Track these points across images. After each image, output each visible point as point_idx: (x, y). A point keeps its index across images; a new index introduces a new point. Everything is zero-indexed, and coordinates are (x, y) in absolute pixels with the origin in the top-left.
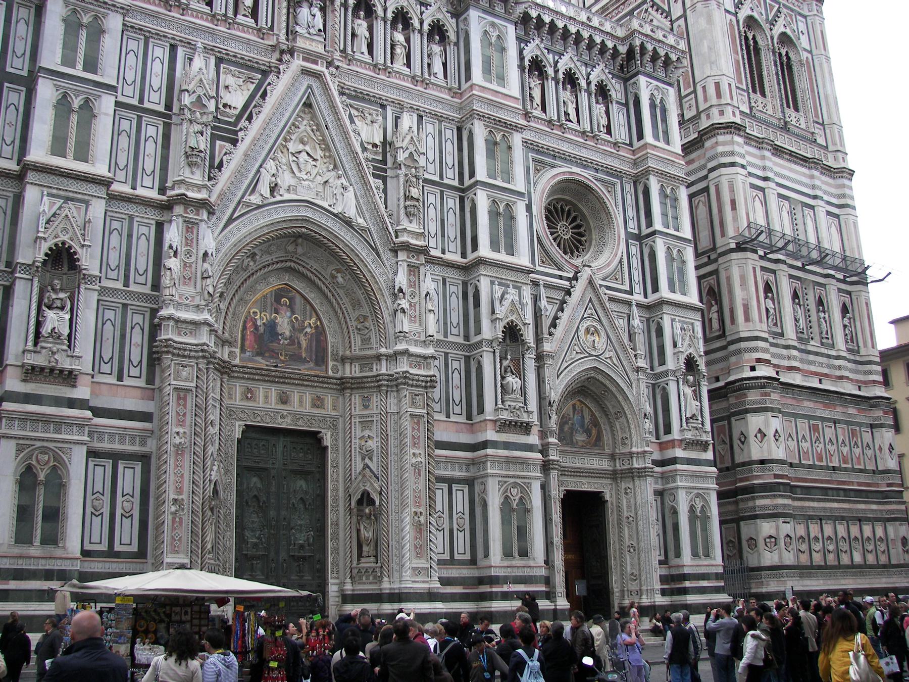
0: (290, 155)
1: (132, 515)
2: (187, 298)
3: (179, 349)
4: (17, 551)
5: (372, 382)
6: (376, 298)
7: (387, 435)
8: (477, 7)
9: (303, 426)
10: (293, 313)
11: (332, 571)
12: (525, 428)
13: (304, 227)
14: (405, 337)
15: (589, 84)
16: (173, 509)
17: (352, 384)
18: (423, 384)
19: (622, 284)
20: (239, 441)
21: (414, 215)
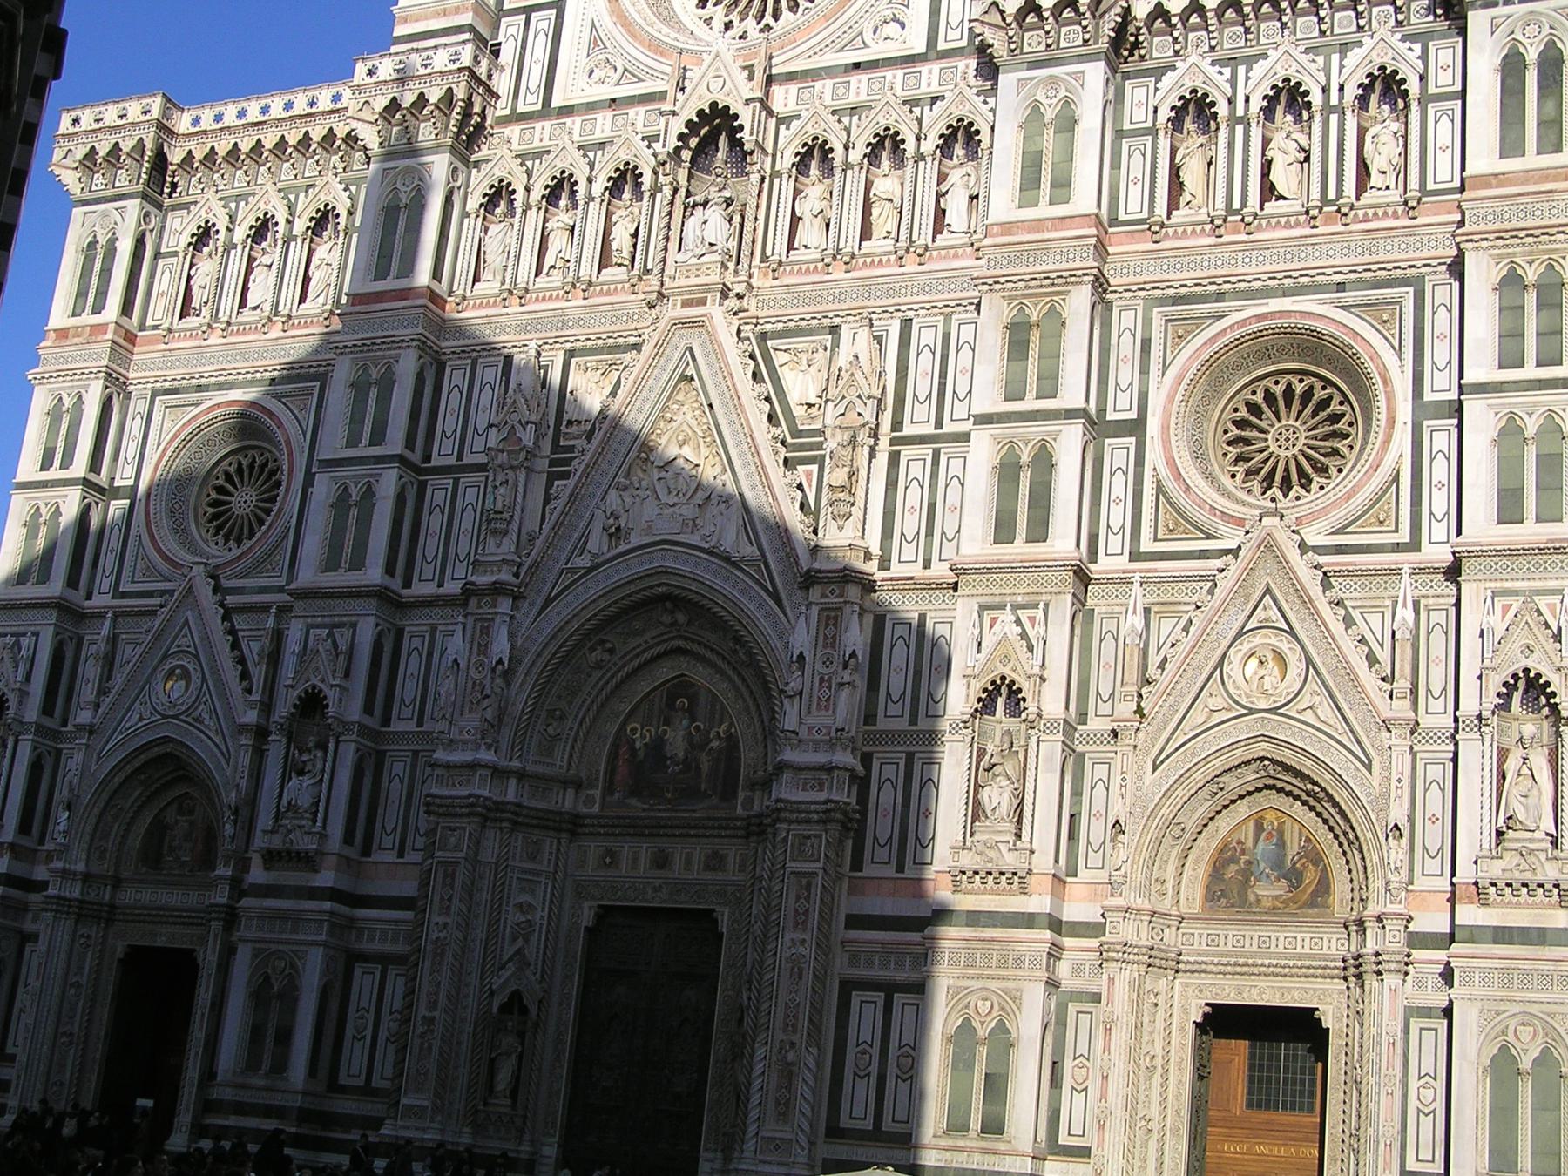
0: (656, 470)
8: (1014, 67)
9: (686, 902)
10: (693, 719)
15: (1341, 88)
16: (421, 1029)
18: (815, 817)
19: (1396, 531)
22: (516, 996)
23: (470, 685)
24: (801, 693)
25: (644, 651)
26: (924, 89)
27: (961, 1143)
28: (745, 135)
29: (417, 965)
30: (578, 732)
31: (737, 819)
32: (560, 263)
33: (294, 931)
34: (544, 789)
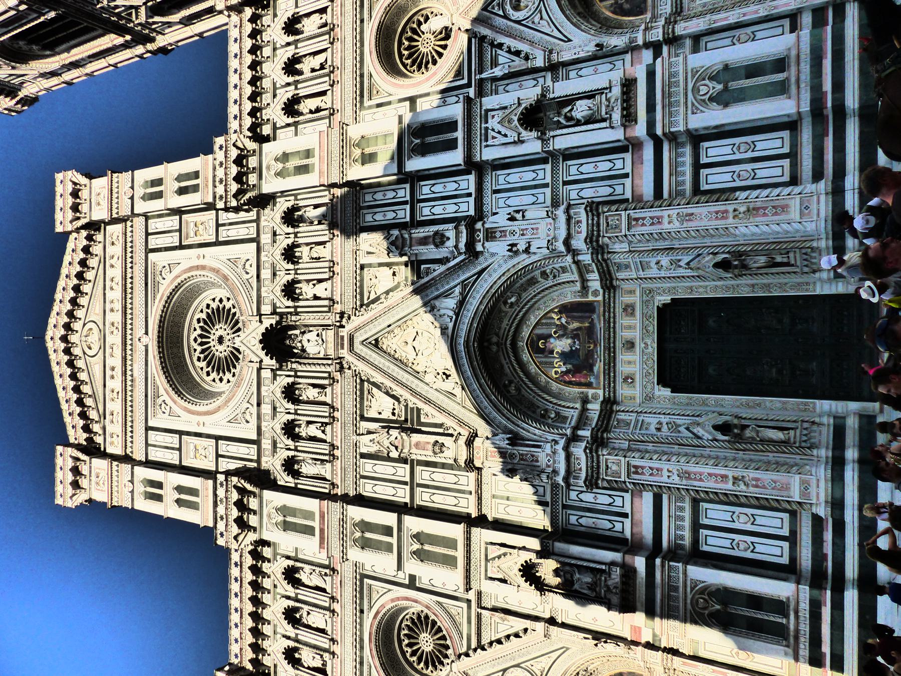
1: (752, 515)
2: (549, 461)
3: (592, 472)
4: (792, 640)
5: (601, 264)
6: (522, 268)
7: (653, 250)
9: (654, 325)
10: (550, 336)
11: (807, 290)
12: (629, 85)
13: (473, 344)
14: (552, 244)
17: (607, 280)
18: (596, 219)
20: (672, 392)
21: (443, 236)
22: (716, 427)
23: (522, 462)
24: (529, 242)
25: (513, 366)
26: (269, 241)
27: (793, 79)
28: (274, 322)
29: (697, 491)
30: (555, 404)
31: (604, 297)
32: (322, 428)
33: (676, 589)
34: (587, 419)
